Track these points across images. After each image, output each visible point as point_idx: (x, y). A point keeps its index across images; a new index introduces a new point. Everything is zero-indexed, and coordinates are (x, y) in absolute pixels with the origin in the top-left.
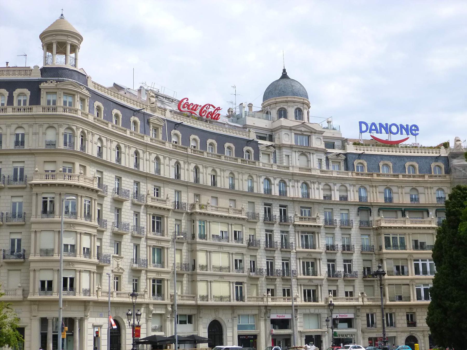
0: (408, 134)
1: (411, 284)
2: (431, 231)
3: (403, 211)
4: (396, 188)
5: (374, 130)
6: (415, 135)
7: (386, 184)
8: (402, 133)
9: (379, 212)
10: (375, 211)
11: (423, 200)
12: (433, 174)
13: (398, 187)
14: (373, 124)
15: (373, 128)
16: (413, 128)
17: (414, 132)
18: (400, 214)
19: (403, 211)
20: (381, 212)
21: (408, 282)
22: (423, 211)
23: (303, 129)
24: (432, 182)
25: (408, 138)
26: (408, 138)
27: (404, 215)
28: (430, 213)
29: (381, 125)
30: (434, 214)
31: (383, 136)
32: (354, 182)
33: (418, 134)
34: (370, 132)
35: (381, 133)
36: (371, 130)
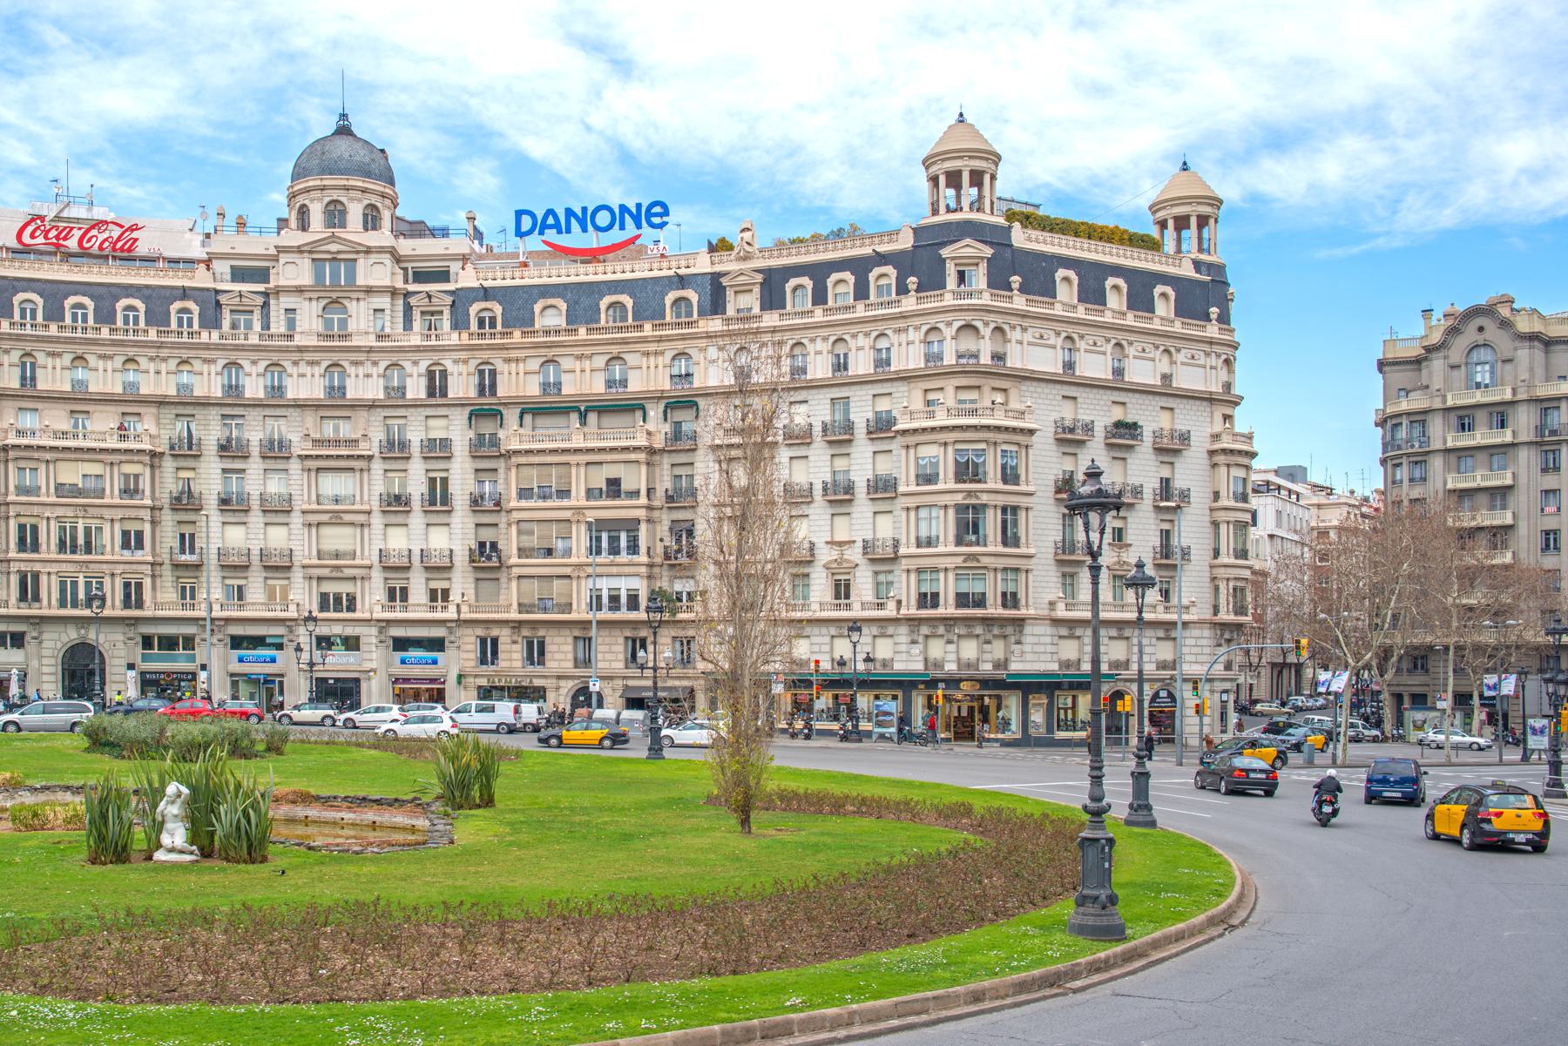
0: (639, 226)
1: (575, 574)
2: (633, 456)
3: (584, 409)
4: (571, 359)
5: (550, 227)
6: (662, 226)
7: (543, 351)
8: (622, 228)
9: (521, 418)
10: (511, 416)
11: (636, 385)
12: (668, 319)
13: (580, 357)
14: (550, 212)
15: (551, 221)
16: (657, 209)
17: (656, 220)
18: (574, 417)
19: (584, 409)
20: (528, 418)
21: (568, 571)
22: (634, 407)
23: (334, 247)
24: (660, 340)
25: (638, 237)
26: (638, 237)
27: (584, 423)
28: (651, 413)
29: (569, 213)
30: (661, 415)
31: (577, 239)
32: (463, 355)
33: (665, 224)
34: (541, 233)
35: (568, 231)
36: (544, 227)
